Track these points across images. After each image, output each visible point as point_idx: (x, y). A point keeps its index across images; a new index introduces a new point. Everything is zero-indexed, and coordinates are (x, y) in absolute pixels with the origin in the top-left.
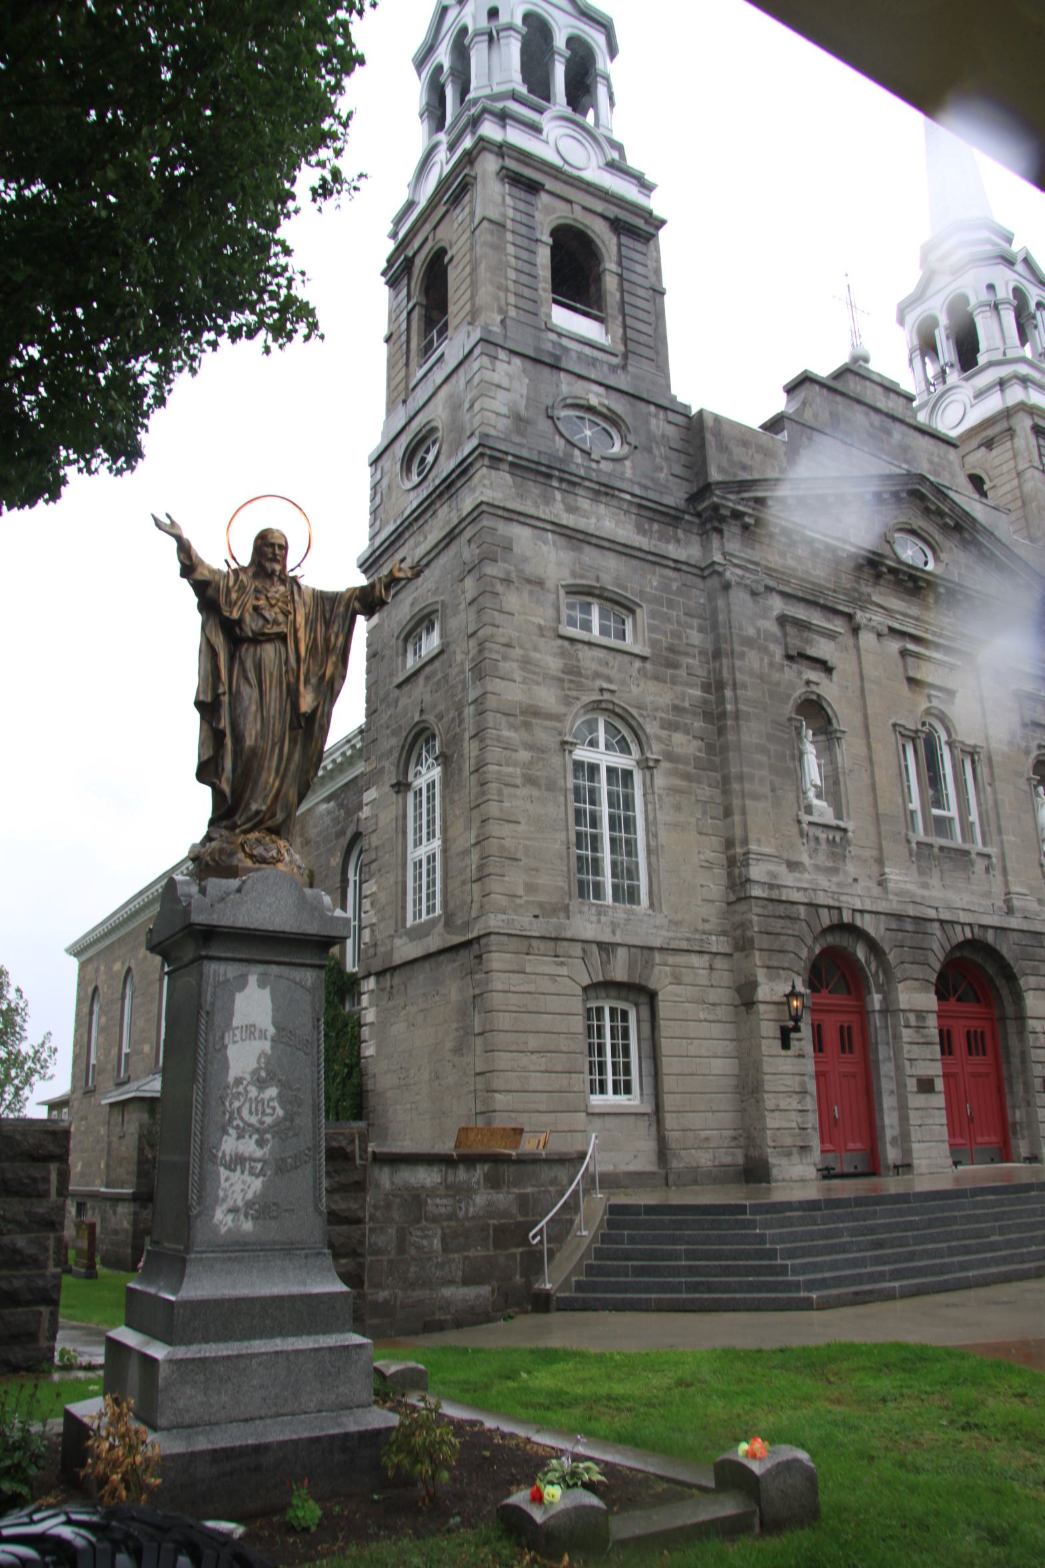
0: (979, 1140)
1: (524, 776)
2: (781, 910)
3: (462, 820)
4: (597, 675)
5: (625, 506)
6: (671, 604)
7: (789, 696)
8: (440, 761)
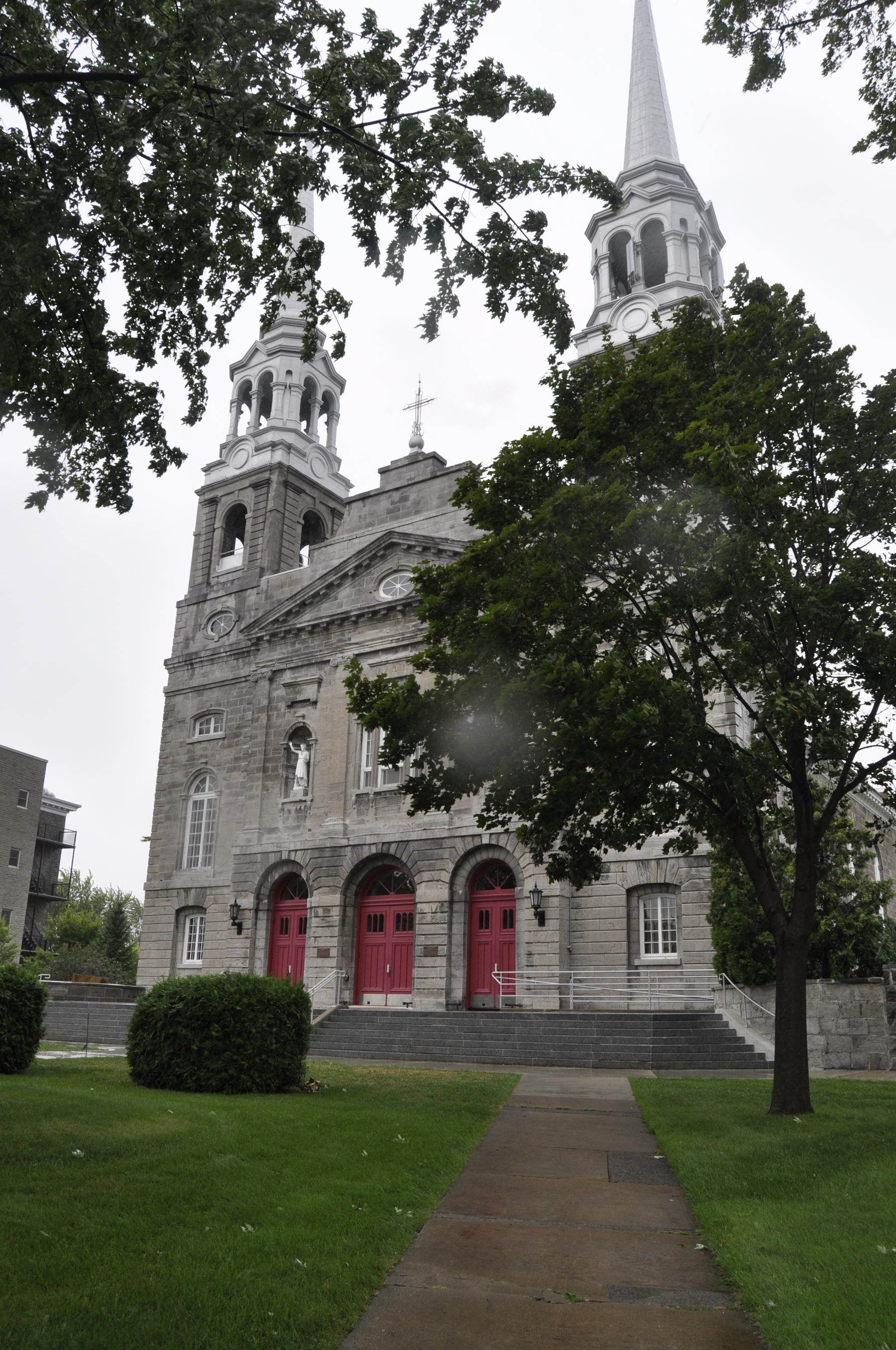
2: (248, 859)
4: (202, 756)
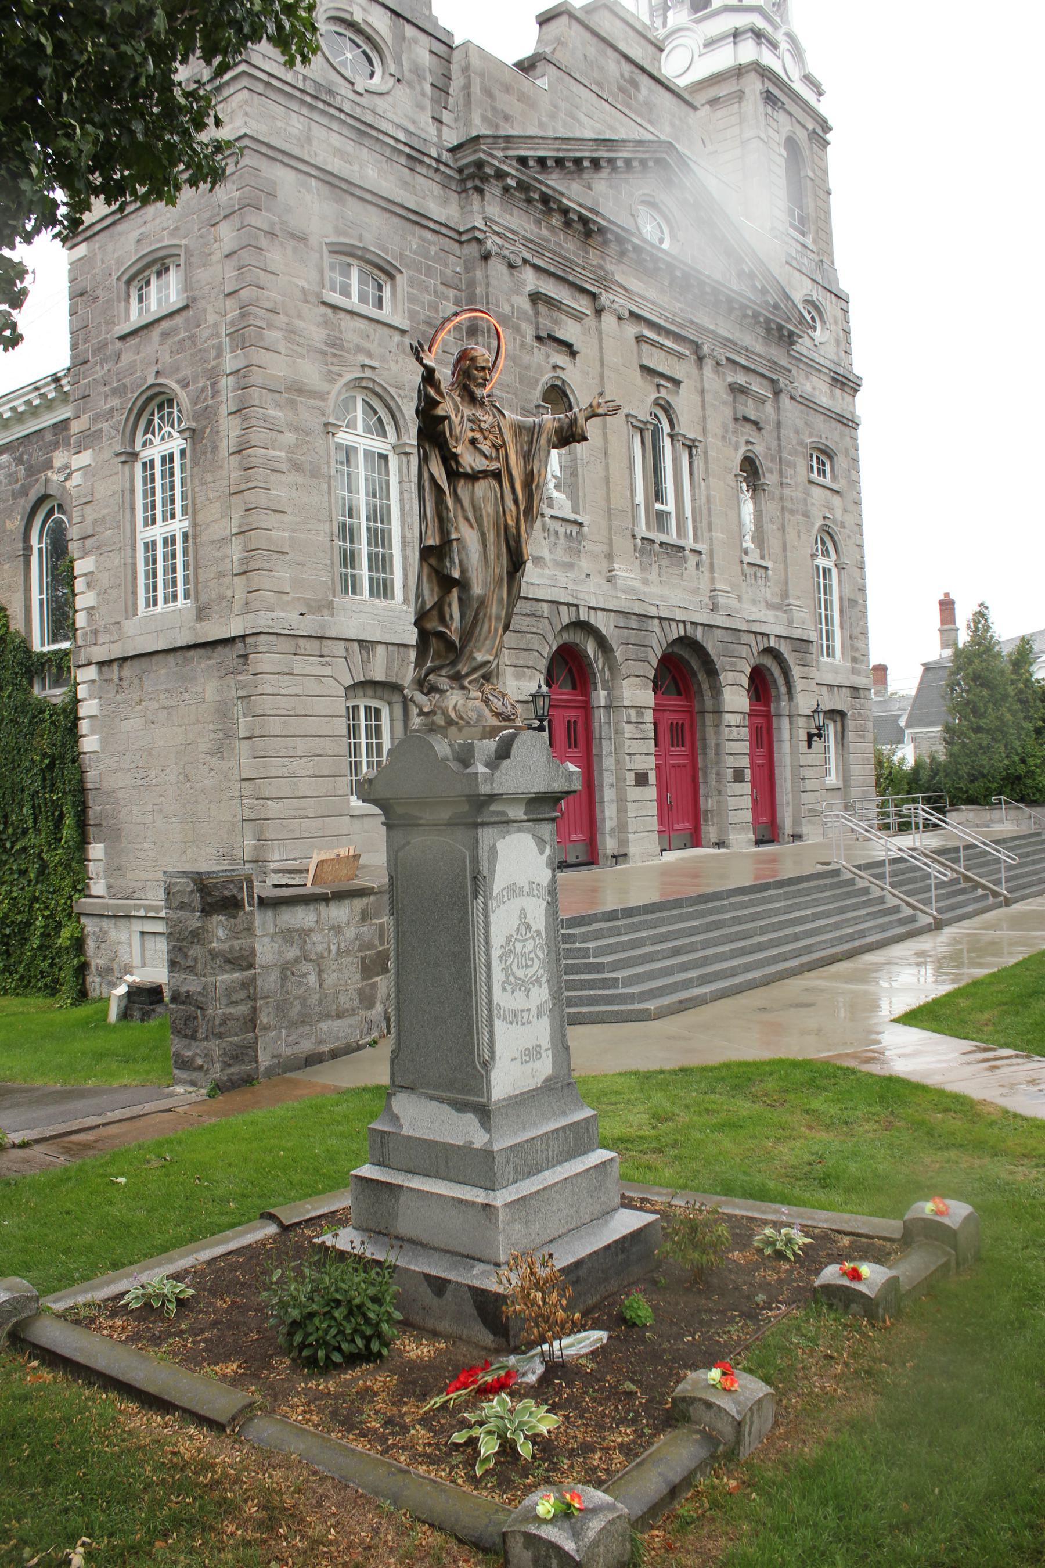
0: (676, 827)
1: (290, 460)
3: (218, 505)
4: (359, 349)
5: (388, 153)
6: (429, 271)
7: (537, 381)
8: (187, 434)
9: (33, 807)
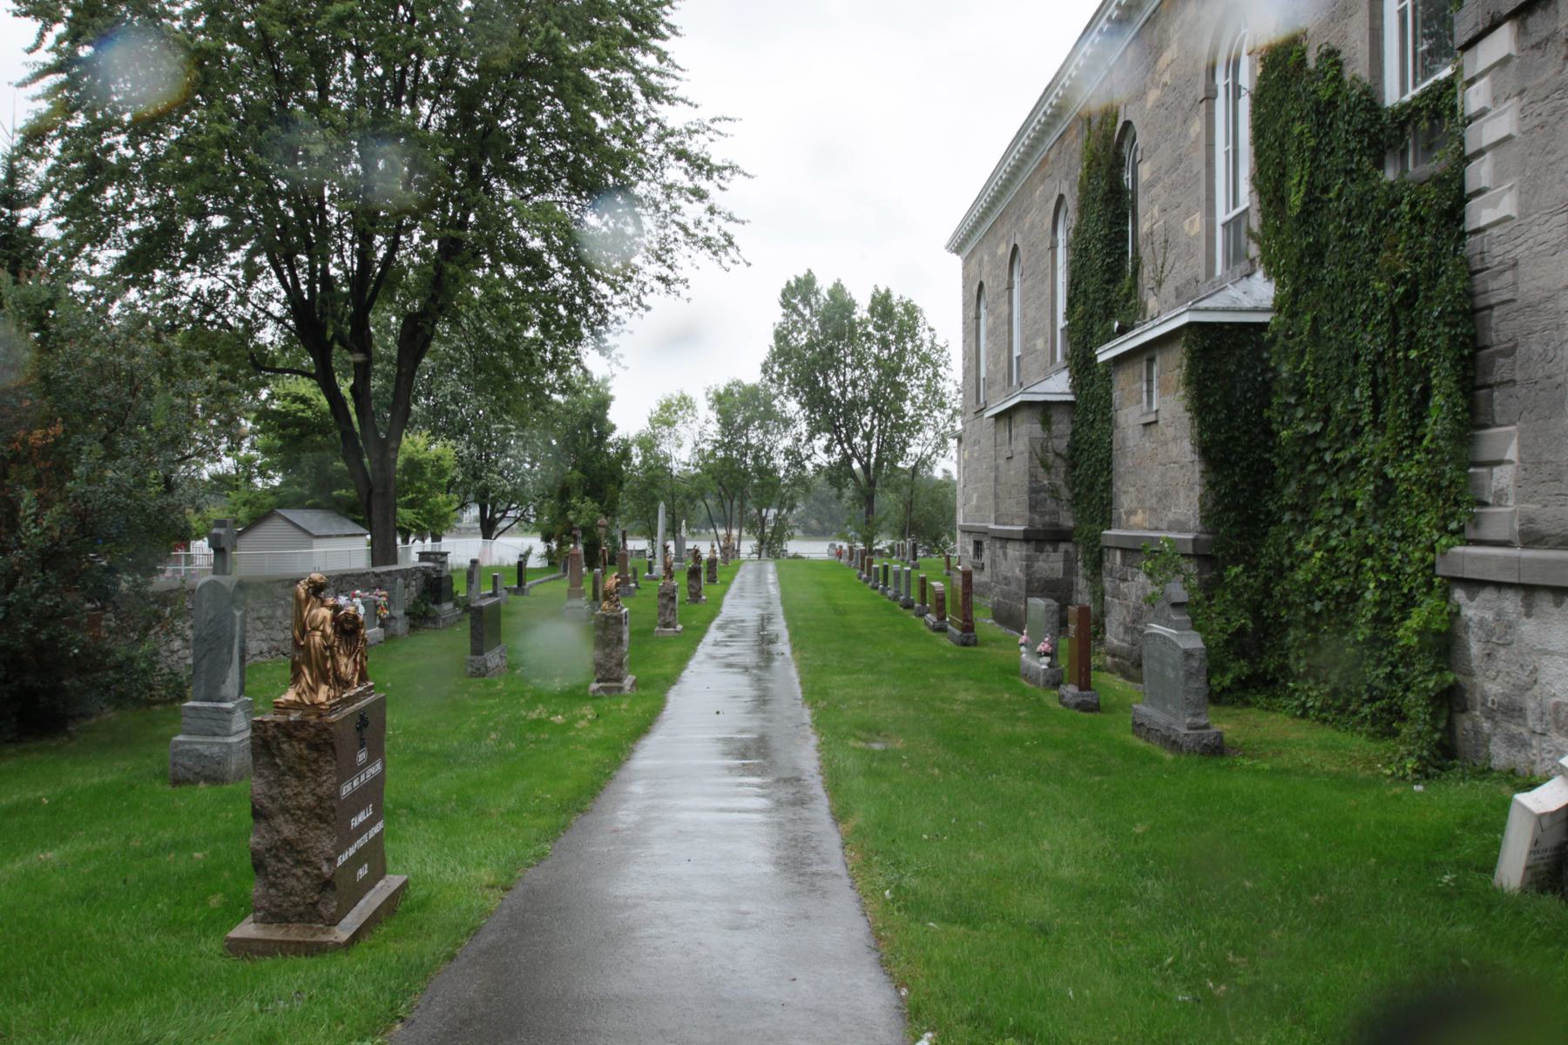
9: (1374, 385)
